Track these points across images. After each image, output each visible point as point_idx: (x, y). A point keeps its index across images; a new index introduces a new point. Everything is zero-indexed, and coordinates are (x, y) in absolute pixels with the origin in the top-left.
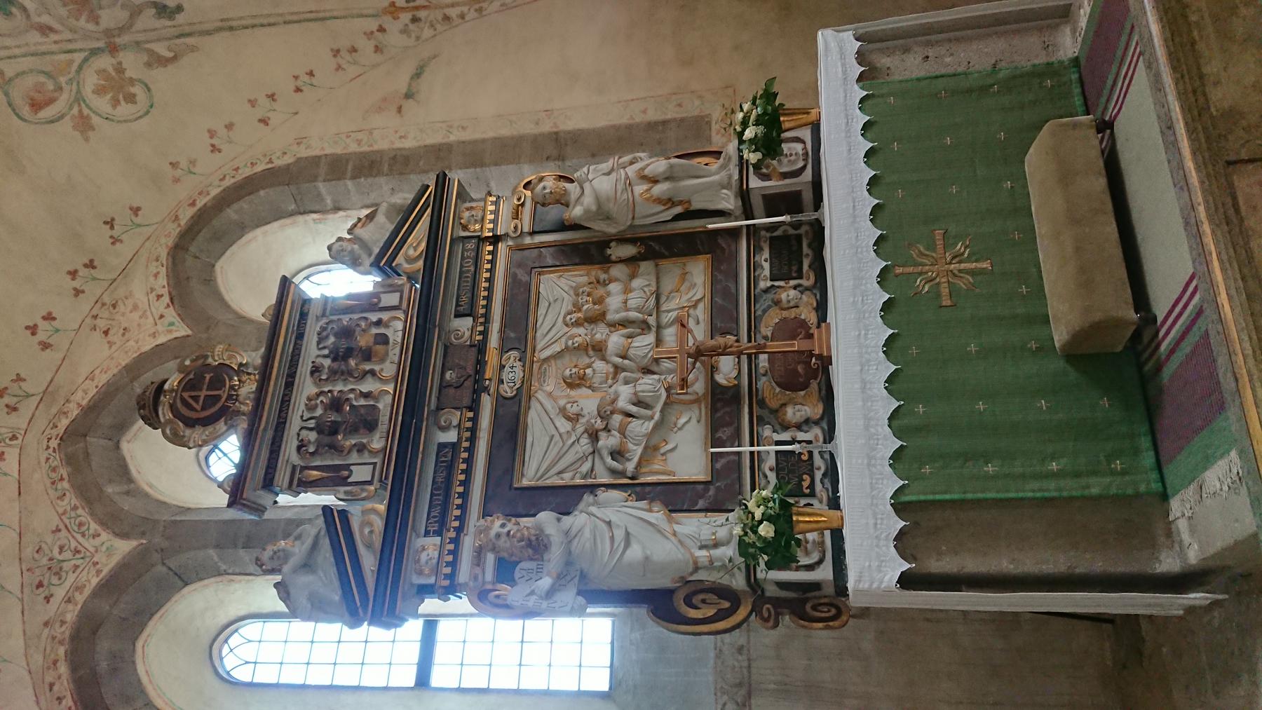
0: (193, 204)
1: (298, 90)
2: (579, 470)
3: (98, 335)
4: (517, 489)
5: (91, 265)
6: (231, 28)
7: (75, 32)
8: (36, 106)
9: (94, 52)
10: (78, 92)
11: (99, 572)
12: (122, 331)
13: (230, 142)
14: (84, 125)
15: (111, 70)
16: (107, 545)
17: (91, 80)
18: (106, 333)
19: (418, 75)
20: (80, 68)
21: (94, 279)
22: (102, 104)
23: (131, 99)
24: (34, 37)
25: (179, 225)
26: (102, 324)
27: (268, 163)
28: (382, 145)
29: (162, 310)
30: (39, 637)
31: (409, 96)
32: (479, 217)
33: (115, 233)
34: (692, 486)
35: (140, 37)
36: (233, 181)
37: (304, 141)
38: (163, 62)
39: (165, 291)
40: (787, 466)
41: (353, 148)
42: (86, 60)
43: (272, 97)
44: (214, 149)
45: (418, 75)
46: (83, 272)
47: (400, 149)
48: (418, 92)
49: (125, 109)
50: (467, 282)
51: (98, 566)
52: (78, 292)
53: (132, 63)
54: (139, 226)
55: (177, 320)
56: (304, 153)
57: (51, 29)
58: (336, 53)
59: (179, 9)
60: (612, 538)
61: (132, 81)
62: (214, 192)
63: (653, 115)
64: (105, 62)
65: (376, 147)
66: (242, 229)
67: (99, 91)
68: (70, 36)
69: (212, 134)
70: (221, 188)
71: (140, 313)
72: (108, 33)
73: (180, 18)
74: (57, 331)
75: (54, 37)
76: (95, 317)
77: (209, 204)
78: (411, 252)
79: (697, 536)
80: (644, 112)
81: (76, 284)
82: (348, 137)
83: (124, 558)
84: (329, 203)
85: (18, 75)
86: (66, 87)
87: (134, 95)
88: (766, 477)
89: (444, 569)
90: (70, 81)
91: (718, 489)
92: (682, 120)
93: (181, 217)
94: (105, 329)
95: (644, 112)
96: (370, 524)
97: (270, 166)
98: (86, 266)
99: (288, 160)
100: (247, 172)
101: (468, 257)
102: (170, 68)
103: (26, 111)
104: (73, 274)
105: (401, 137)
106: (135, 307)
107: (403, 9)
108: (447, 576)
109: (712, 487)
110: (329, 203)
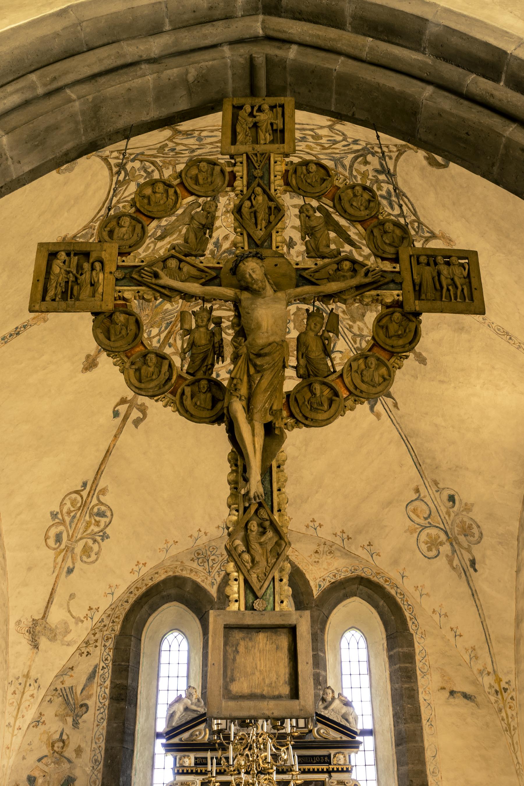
3: (315, 547)
5: (349, 538)
6: (473, 595)
7: (452, 525)
8: (414, 511)
9: (446, 533)
10: (426, 527)
11: (203, 581)
12: (317, 560)
13: (421, 596)
15: (439, 540)
16: (215, 583)
18: (317, 552)
20: (437, 527)
21: (343, 540)
22: (423, 537)
23: (429, 549)
26: (321, 549)
28: (421, 681)
30: (177, 561)
32: (339, 763)
35: (458, 552)
38: (450, 562)
42: (442, 529)
46: (345, 536)
47: (418, 692)
48: (454, 698)
49: (424, 547)
50: (308, 760)
51: (206, 580)
52: (335, 535)
54: (372, 557)
55: (322, 588)
57: (449, 516)
58: (473, 649)
59: (476, 570)
68: (450, 523)
70: (395, 595)
71: (326, 567)
72: (456, 539)
73: (471, 570)
74: (315, 529)
75: (447, 518)
76: (325, 544)
77: (386, 590)
78: (322, 731)
83: (208, 592)
85: (425, 503)
87: (431, 550)
90: (429, 523)
94: (318, 551)
96: (200, 734)
97: (408, 619)
98: (348, 536)
101: (320, 759)
102: (448, 567)
104: (343, 532)
106: (329, 564)
107: (499, 686)
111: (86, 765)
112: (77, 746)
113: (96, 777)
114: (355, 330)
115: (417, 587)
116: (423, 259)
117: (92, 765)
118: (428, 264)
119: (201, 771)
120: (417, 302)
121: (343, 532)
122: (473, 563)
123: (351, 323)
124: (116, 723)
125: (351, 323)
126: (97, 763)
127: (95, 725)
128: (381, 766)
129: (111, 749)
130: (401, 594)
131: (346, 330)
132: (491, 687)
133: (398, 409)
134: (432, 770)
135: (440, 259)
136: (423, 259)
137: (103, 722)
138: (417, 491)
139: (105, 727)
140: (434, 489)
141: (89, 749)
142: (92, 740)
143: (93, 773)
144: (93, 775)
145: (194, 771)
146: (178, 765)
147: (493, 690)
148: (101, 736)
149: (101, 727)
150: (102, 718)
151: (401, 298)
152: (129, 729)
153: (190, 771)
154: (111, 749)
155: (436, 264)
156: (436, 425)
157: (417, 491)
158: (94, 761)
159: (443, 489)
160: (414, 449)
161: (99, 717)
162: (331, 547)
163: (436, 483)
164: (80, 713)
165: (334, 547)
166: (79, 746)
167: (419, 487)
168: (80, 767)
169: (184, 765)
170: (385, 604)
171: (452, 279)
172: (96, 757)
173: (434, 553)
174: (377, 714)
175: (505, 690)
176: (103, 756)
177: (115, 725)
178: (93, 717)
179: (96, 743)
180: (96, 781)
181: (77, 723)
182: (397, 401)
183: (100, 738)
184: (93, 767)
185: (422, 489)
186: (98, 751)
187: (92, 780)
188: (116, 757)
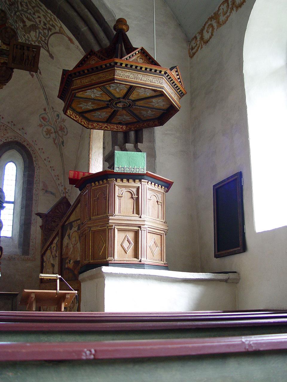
0: (27, 145)
1: (51, 167)
5: (14, 125)
8: (43, 118)
14: (41, 126)
15: (51, 131)
17: (49, 128)
19: (52, 193)
22: (45, 129)
23: (47, 134)
24: (55, 120)
25: (22, 142)
27: (35, 160)
29: (3, 141)
31: (46, 191)
33: (21, 129)
36: (32, 153)
37: (39, 169)
38: (54, 141)
39: (7, 141)
41: (35, 180)
42: (53, 127)
43: (49, 162)
44: (39, 149)
45: (52, 193)
46: (13, 124)
49: (45, 133)
52: (9, 123)
53: (53, 135)
54: (23, 134)
56: (36, 170)
57: (56, 122)
58: (58, 176)
59: (63, 146)
61: (50, 135)
62: (30, 149)
63: (31, 244)
64: (53, 130)
65: (34, 184)
66: (22, 155)
67: (47, 129)
68: (56, 125)
69: (42, 149)
72: (58, 132)
73: (62, 145)
75: (55, 123)
80: (33, 242)
81: (10, 122)
82: (38, 178)
84: (25, 173)
85: (48, 115)
86: (47, 123)
87: (47, 135)
90: (48, 124)
92: (29, 250)
93: (25, 143)
95: (33, 242)
97: (34, 161)
98: (14, 124)
99: (35, 165)
100: (33, 156)
103: (41, 116)
104: (12, 122)
105: (36, 190)
106: (4, 134)
107: (65, 191)
110: (25, 173)
114: (26, 37)
115: (40, 149)
116: (19, 47)
118: (20, 49)
120: (13, 64)
121: (12, 122)
122: (63, 142)
123: (25, 34)
125: (25, 34)
128: (15, 215)
130: (33, 151)
131: (22, 36)
132: (62, 191)
133: (41, 75)
134: (33, 219)
135: (25, 48)
136: (19, 47)
138: (45, 110)
140: (52, 110)
147: (63, 192)
151: (7, 62)
155: (23, 49)
156: (55, 85)
157: (45, 110)
159: (56, 111)
160: (46, 92)
162: (6, 127)
163: (53, 108)
165: (7, 128)
167: (46, 109)
170: (25, 154)
171: (28, 57)
173: (48, 136)
174: (16, 196)
175: (67, 192)
182: (41, 71)
185: (47, 109)
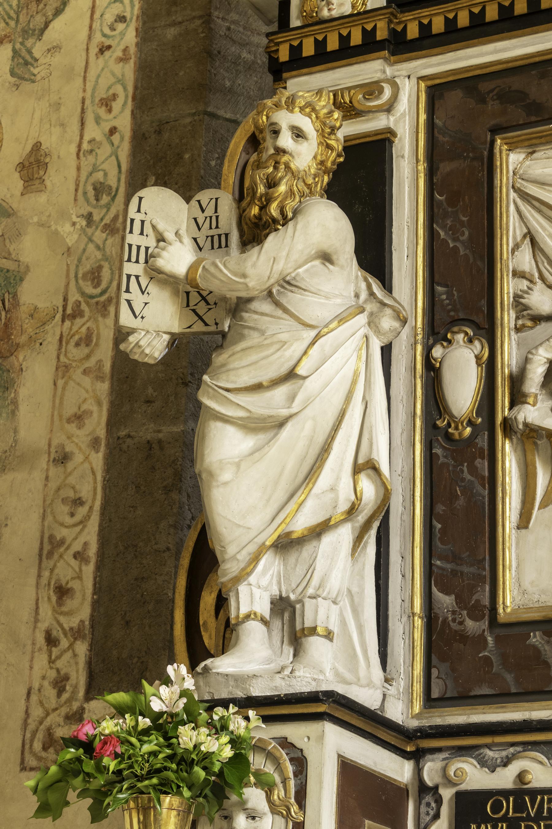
2: (540, 284)
4: (493, 143)
34: (487, 573)
40: (529, 818)
60: (258, 387)
79: (311, 591)
88: (506, 763)
89: (312, 40)
91: (481, 640)
108: (296, 51)
109: (484, 624)
111: (63, 215)
112: (29, 148)
113: (99, 255)
117: (86, 209)
119: (425, 29)
124: (174, 24)
126: (105, 199)
127: (94, 50)
129: (159, 132)
137: (123, 34)
139: (133, 50)
141: (73, 149)
142: (83, 111)
143: (90, 240)
144: (91, 247)
145: (382, 34)
146: (295, 22)
148: (119, 89)
149: (119, 53)
150: (121, 19)
152: (244, 45)
153: (356, 39)
154: (159, 132)
158: (91, 193)
161: (109, 18)
164: (39, 20)
166: (37, 146)
168: (41, 225)
169: (325, 13)
172: (99, 176)
176: (124, 167)
177: (171, 33)
178: (87, 21)
179: (98, 120)
180: (100, 268)
181: (26, 63)
183: (114, 97)
184: (89, 217)
186: (105, 150)
187: (87, 266)
188: (180, 156)
